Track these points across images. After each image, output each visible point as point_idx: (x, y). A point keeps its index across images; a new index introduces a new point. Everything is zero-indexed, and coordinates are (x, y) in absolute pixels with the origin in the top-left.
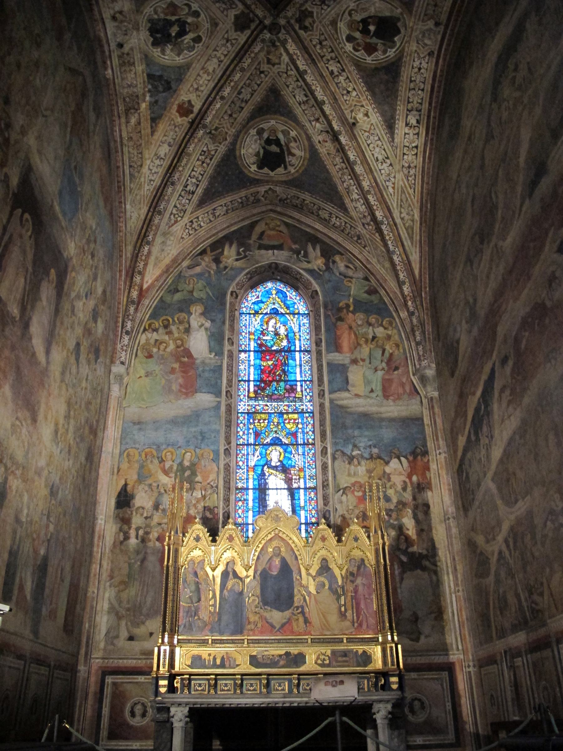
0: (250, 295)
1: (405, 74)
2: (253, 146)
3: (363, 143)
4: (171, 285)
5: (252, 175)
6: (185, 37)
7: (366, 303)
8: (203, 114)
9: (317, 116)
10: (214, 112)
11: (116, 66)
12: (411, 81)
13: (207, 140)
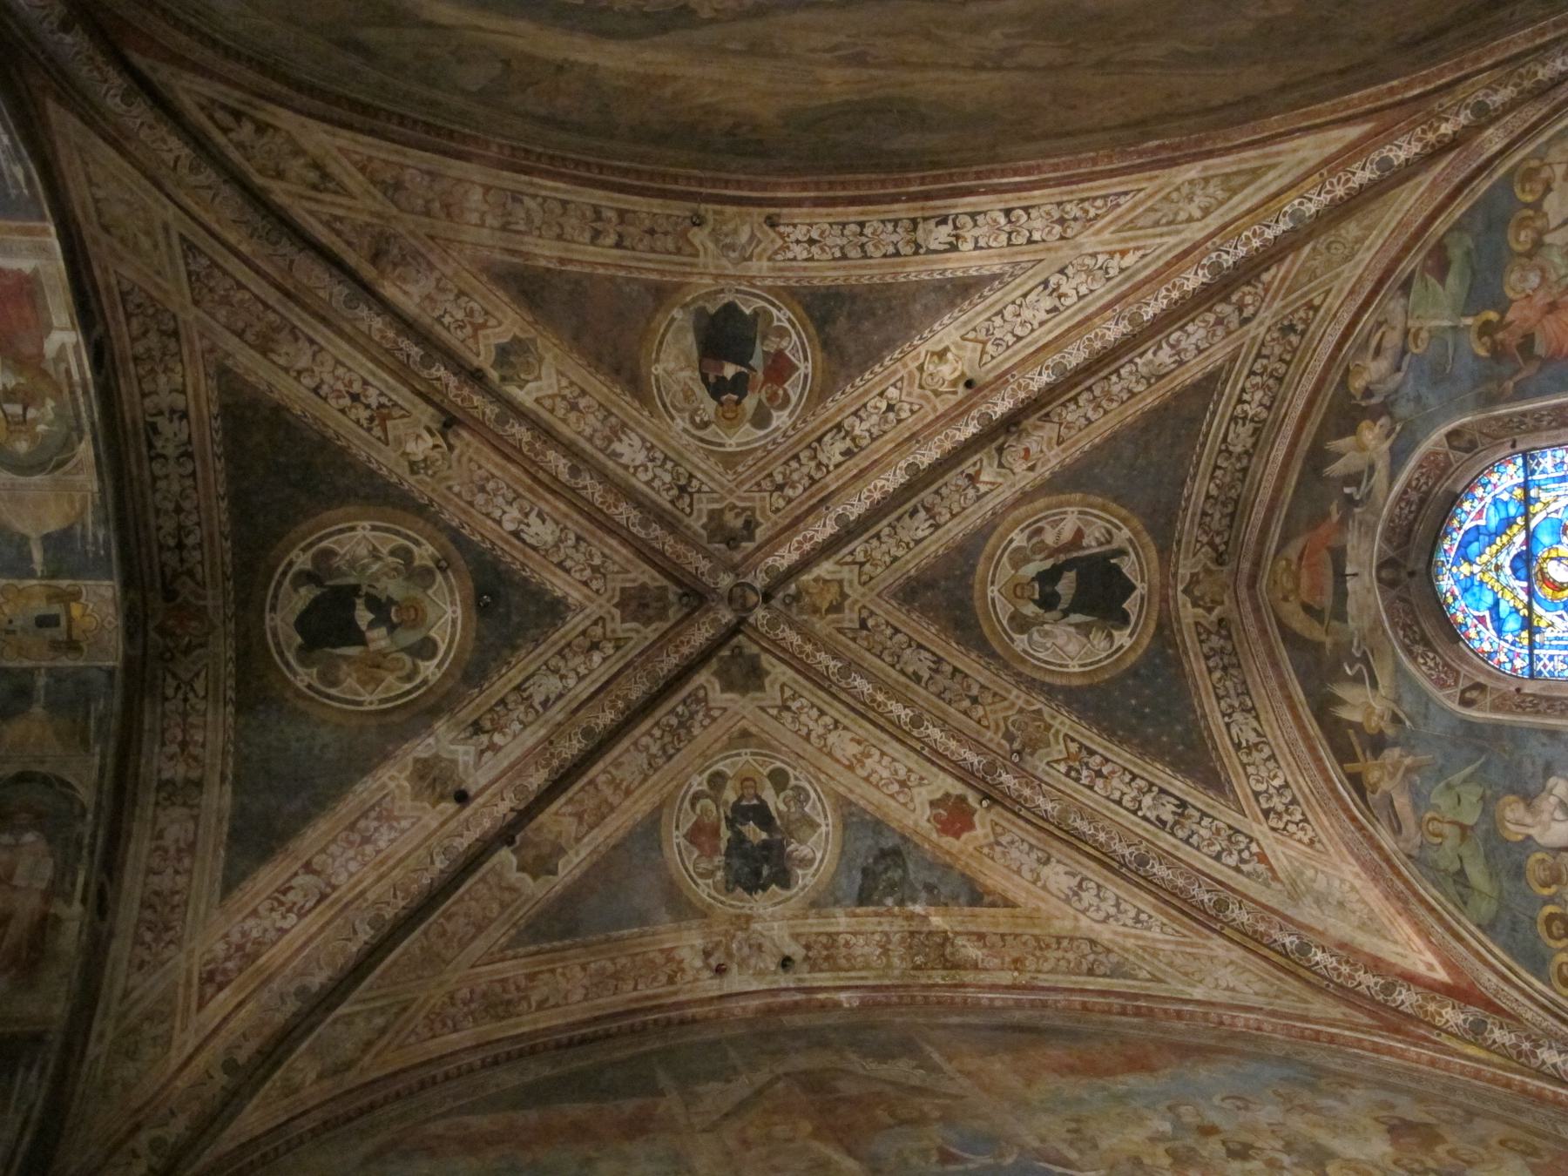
0: (1477, 644)
1: (829, 275)
2: (1061, 641)
3: (1015, 354)
4: (1444, 893)
5: (1146, 641)
6: (772, 808)
7: (1474, 273)
8: (963, 773)
9: (963, 482)
10: (953, 744)
11: (834, 979)
12: (844, 257)
13: (1038, 764)
